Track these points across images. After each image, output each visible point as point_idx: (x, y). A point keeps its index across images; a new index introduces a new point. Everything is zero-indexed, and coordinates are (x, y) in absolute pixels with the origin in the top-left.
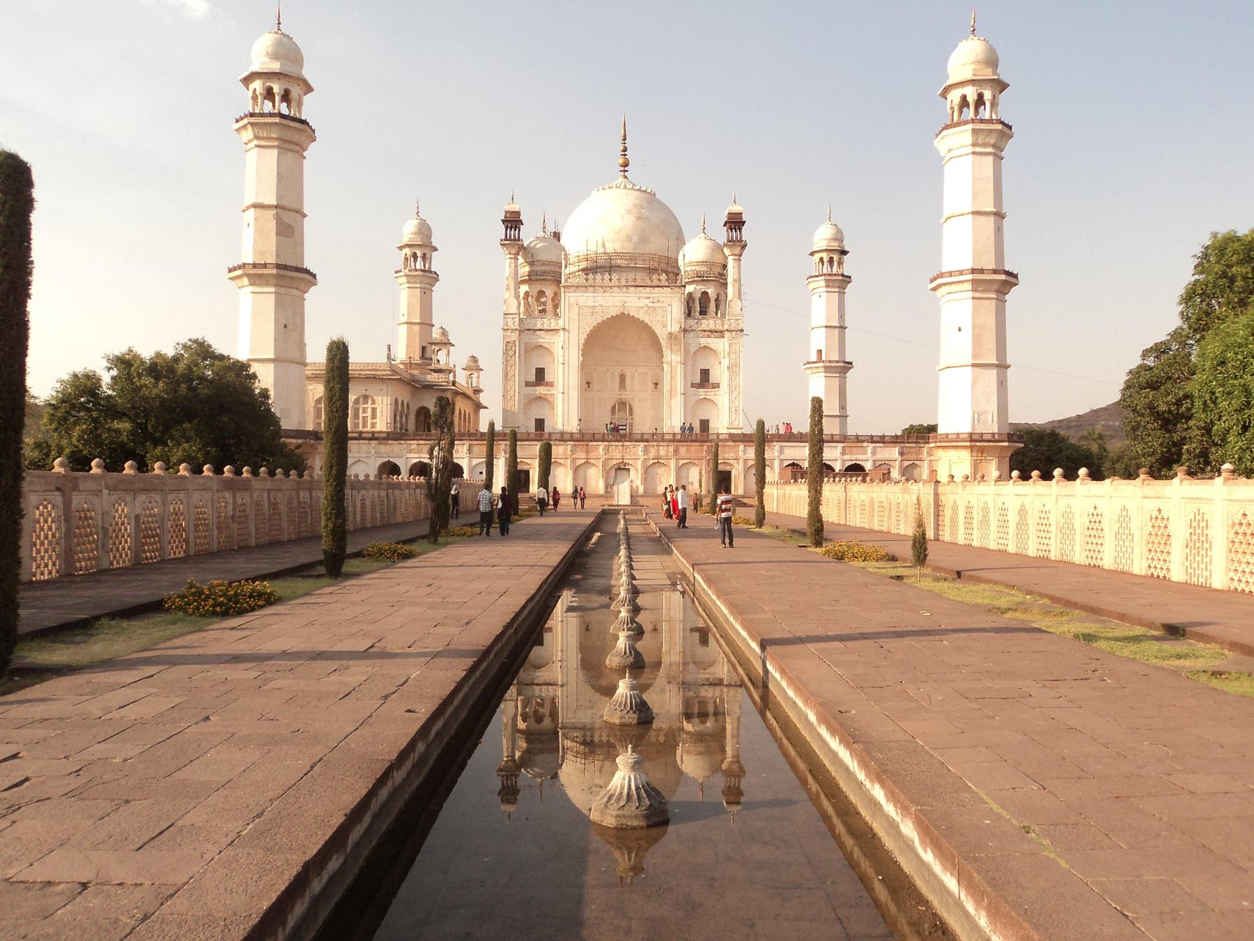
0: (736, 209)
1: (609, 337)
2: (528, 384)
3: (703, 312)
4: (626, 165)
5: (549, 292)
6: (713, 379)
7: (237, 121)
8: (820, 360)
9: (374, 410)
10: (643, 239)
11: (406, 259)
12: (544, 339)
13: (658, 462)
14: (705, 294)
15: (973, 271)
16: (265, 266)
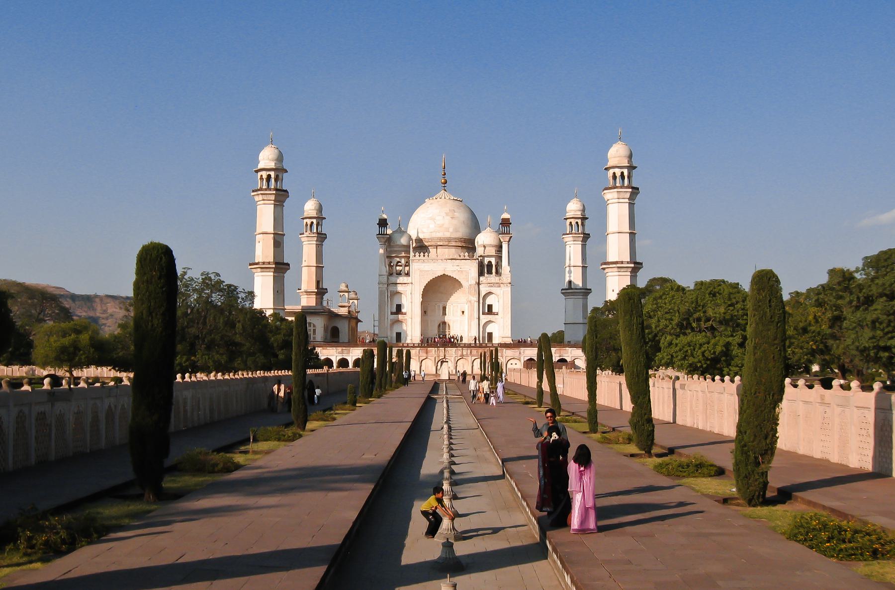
0: (506, 216)
1: (438, 289)
2: (392, 313)
3: (490, 272)
4: (446, 182)
5: (403, 261)
6: (494, 310)
7: (253, 191)
8: (570, 287)
9: (314, 331)
10: (456, 230)
11: (307, 225)
12: (400, 288)
13: (462, 357)
14: (490, 262)
15: (616, 263)
16: (269, 263)
